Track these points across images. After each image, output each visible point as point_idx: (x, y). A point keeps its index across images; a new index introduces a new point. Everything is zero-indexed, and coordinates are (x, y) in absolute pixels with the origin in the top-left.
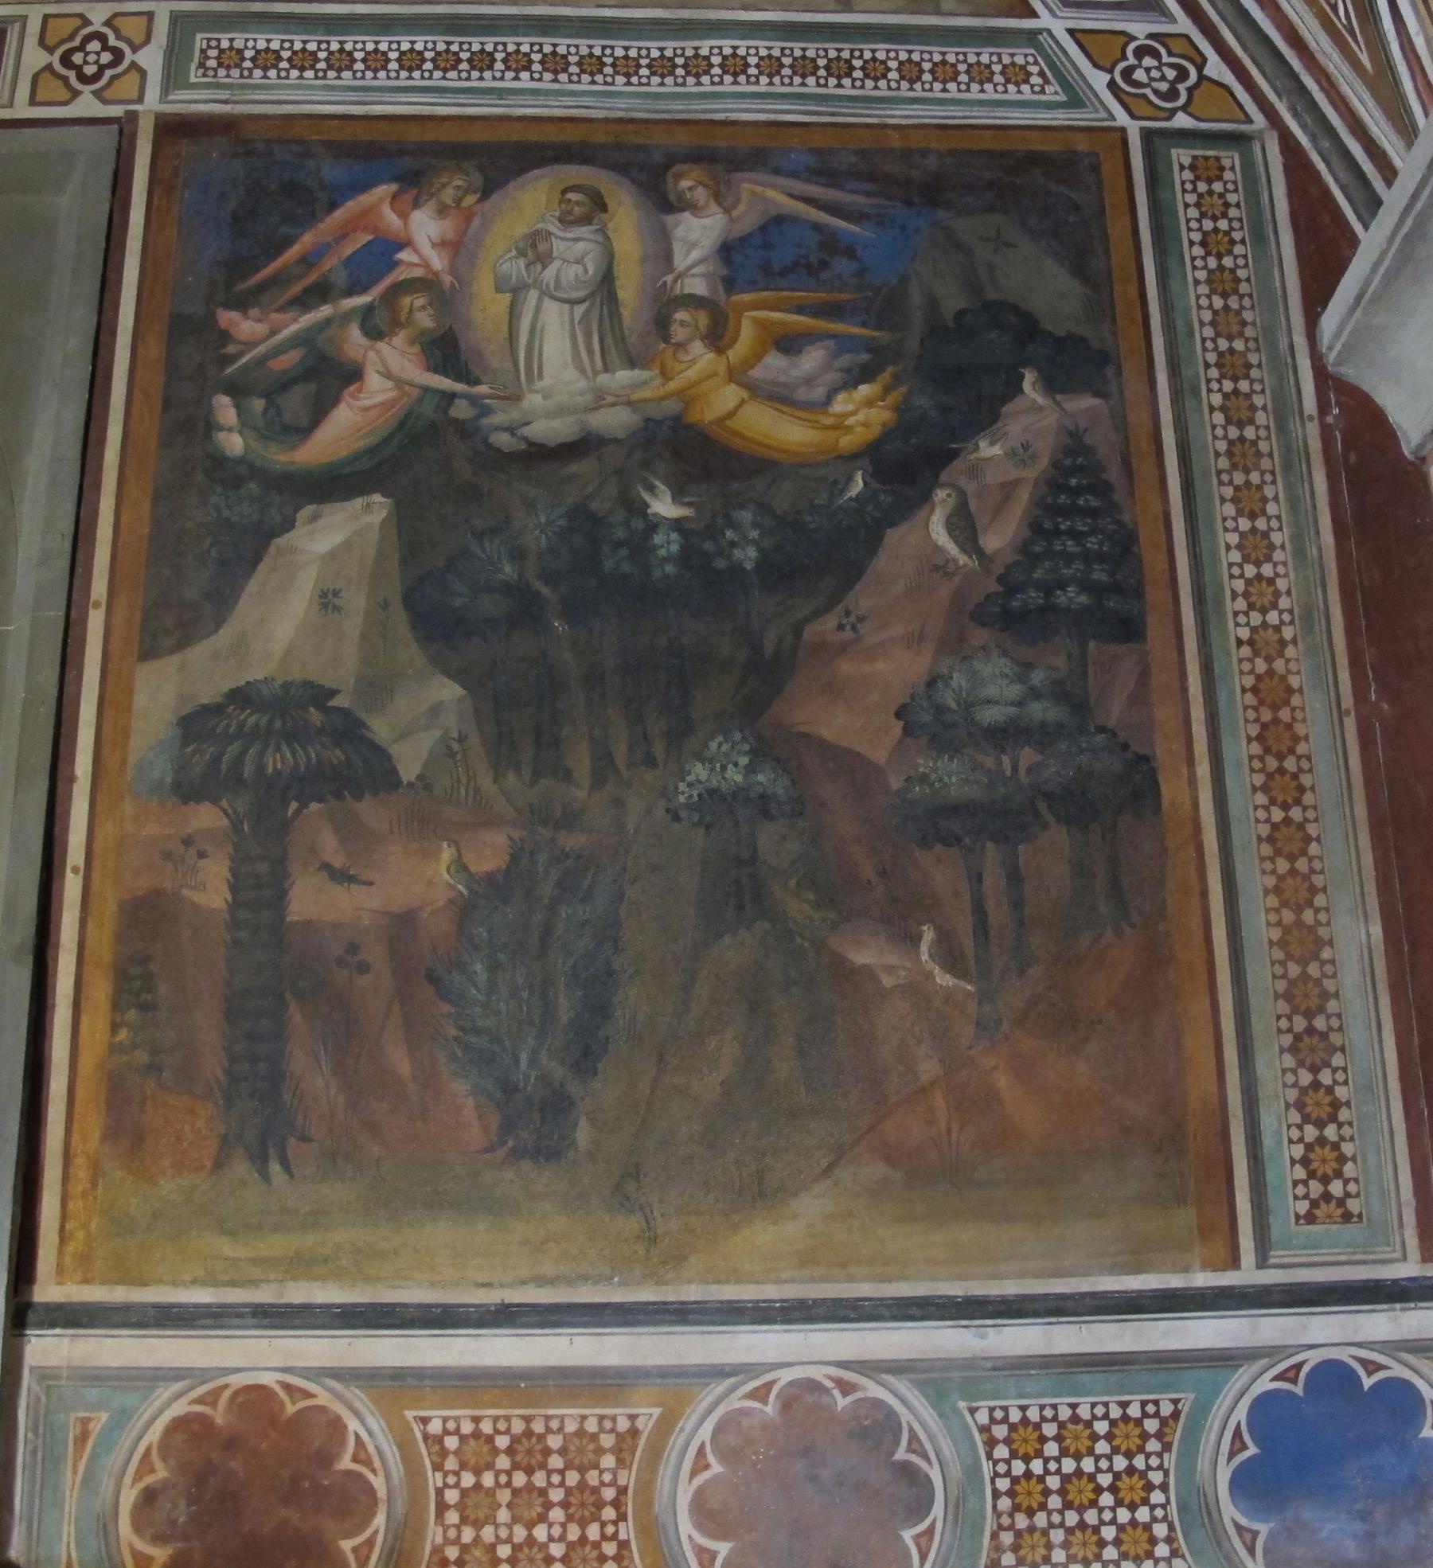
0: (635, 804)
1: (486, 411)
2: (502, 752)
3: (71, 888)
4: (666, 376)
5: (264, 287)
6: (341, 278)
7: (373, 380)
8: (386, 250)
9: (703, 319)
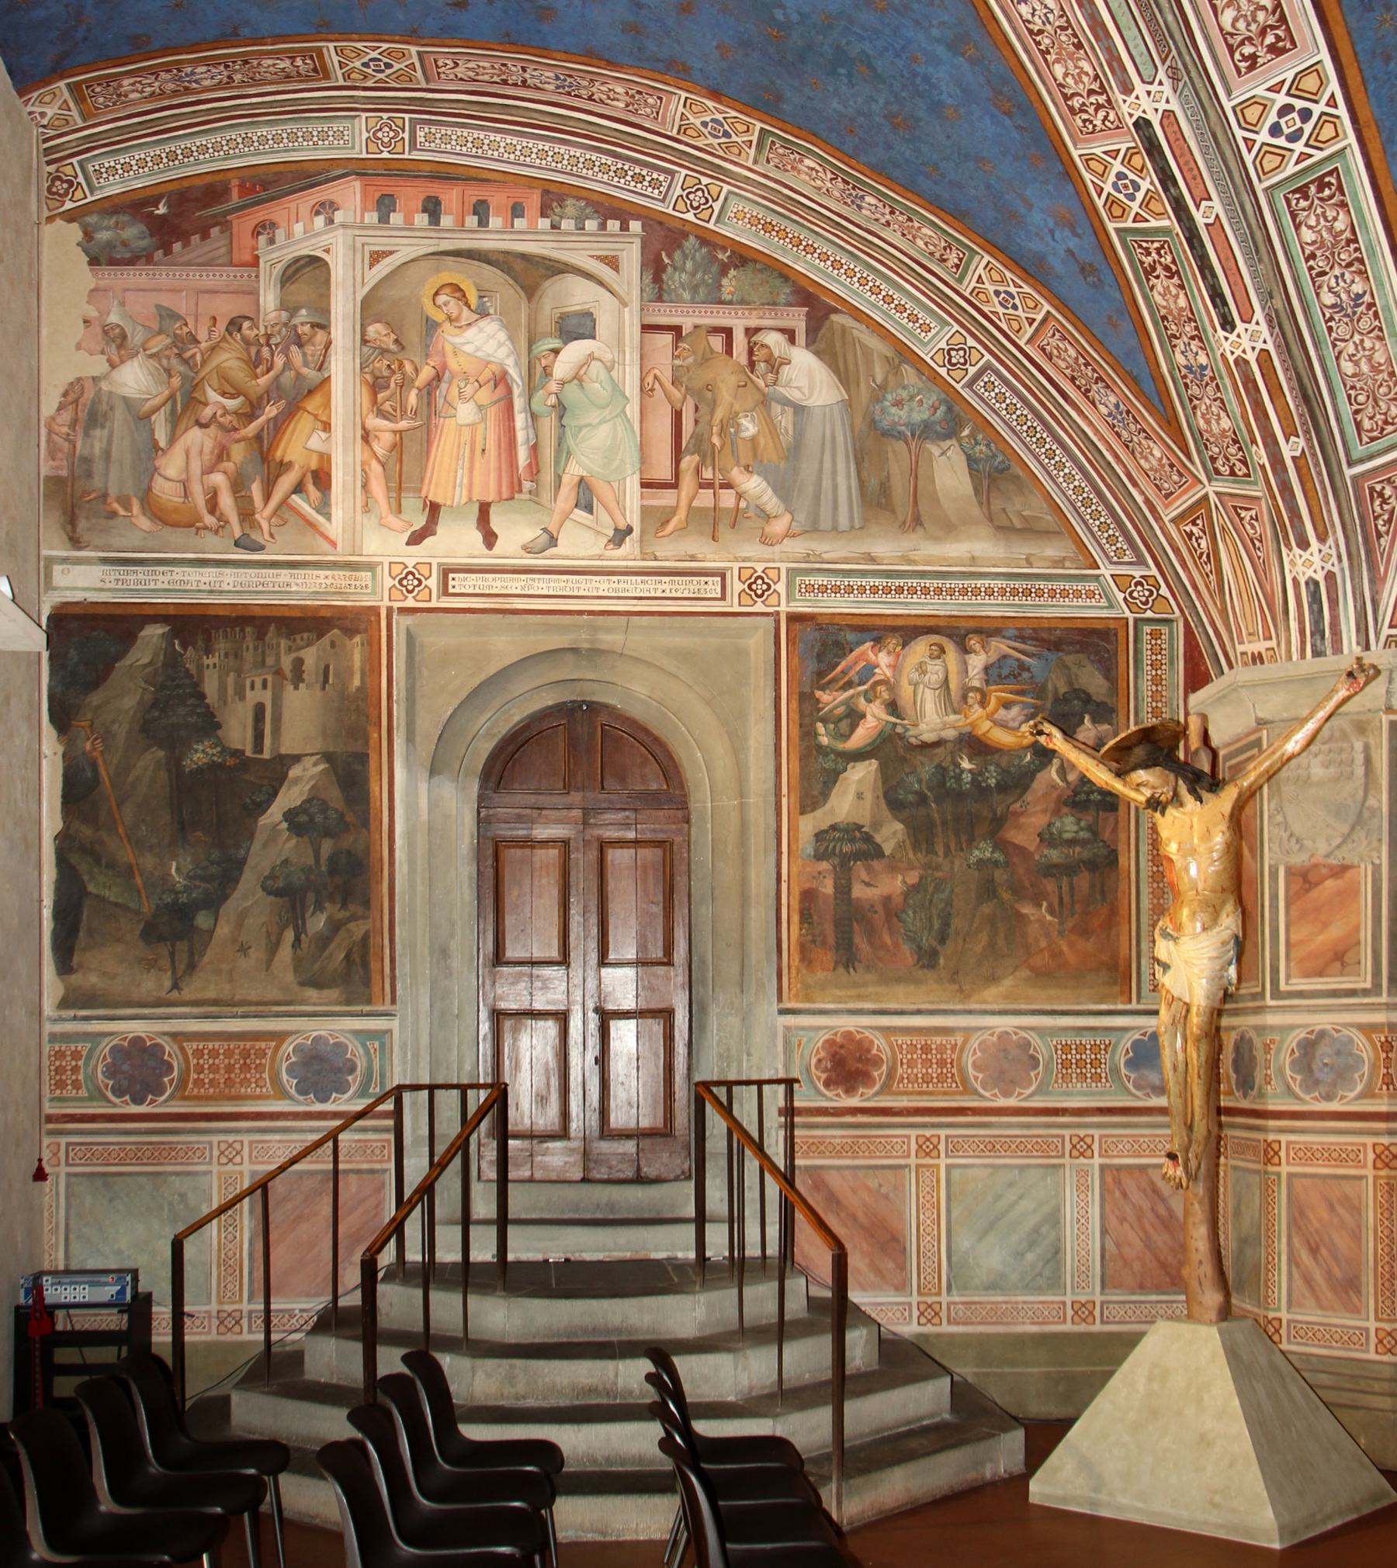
0: (957, 863)
1: (907, 730)
2: (916, 846)
3: (784, 886)
4: (966, 717)
5: (829, 682)
6: (856, 679)
7: (869, 717)
8: (871, 668)
9: (979, 697)
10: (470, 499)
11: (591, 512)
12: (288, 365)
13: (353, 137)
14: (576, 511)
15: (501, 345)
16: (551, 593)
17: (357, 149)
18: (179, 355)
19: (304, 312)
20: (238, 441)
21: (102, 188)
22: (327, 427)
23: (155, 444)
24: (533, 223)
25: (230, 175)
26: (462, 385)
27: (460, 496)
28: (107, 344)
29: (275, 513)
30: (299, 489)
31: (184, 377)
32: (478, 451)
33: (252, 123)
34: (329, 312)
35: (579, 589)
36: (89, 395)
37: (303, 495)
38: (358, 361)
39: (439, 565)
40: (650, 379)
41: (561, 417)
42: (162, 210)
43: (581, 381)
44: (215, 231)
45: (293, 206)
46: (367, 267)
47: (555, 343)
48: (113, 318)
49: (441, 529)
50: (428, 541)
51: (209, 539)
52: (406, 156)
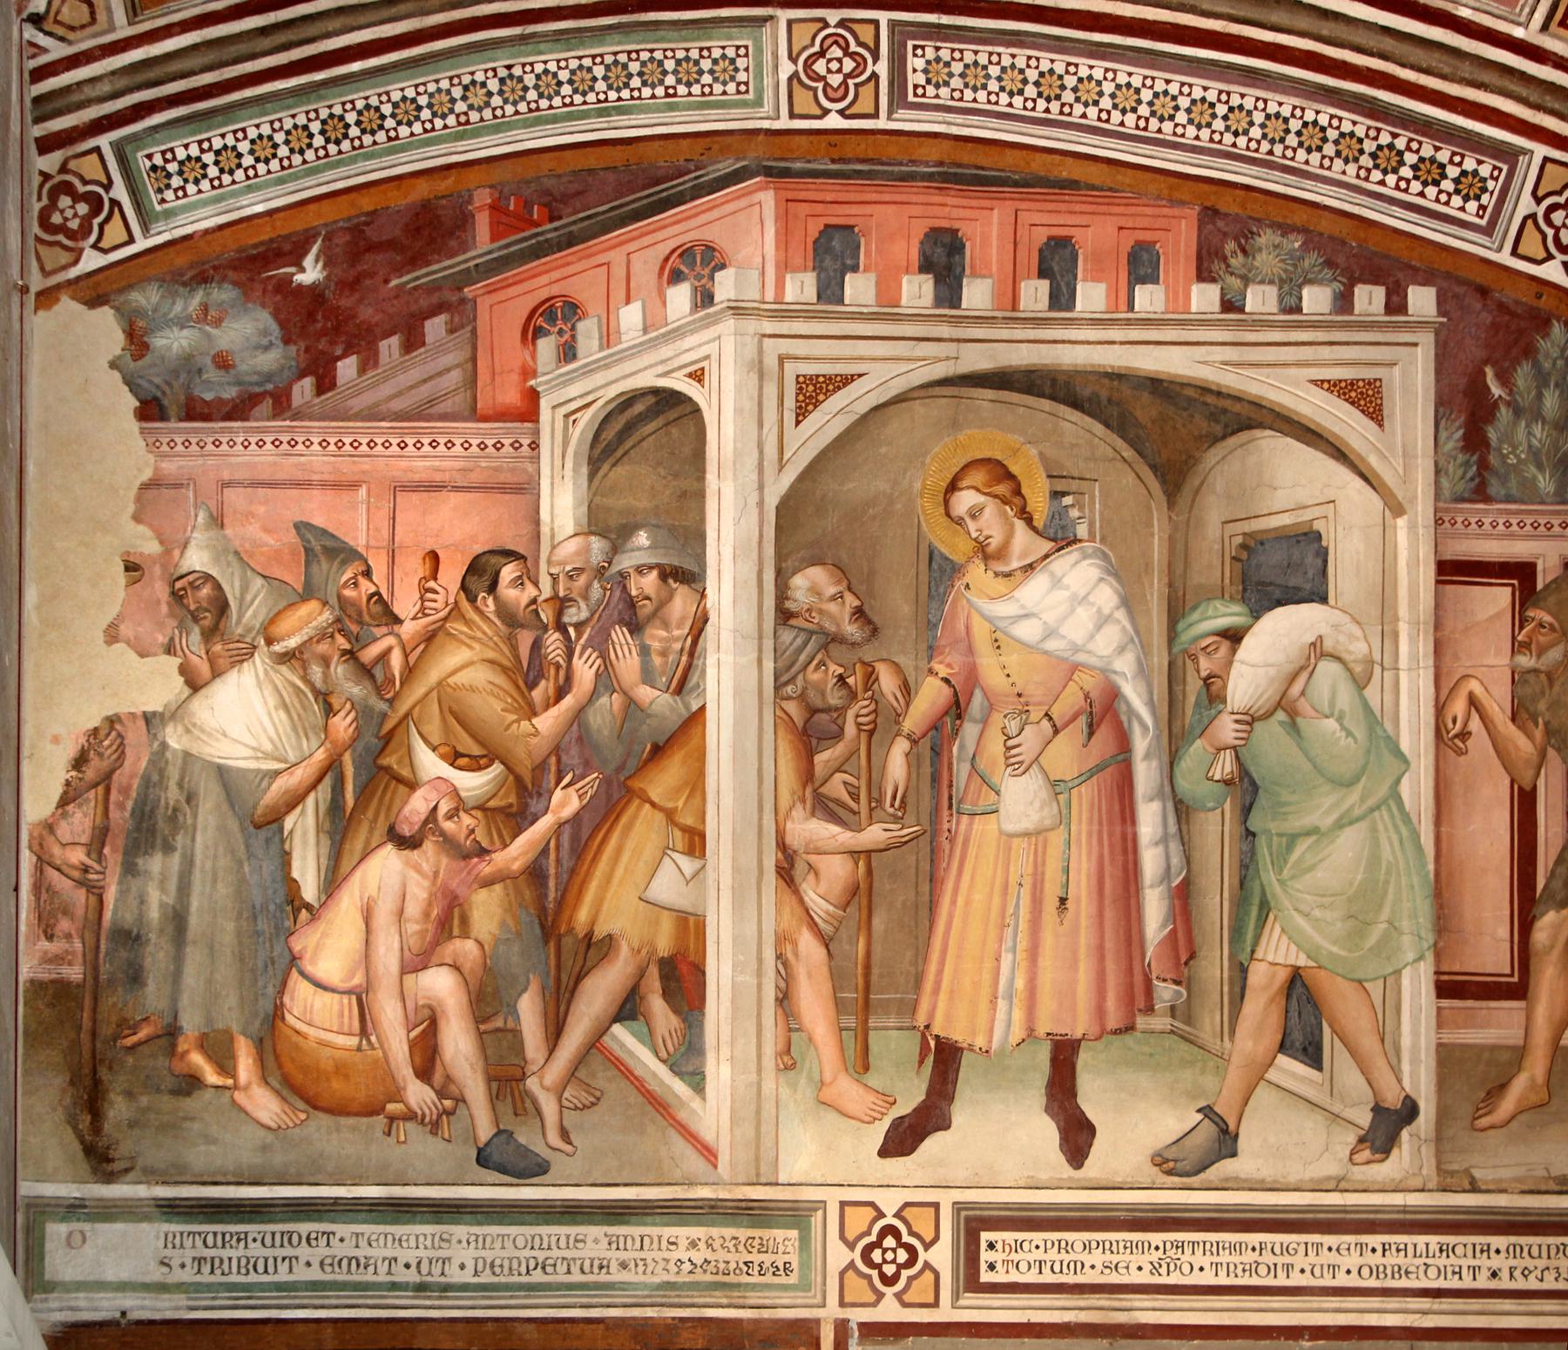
10: (1031, 1031)
11: (1317, 1063)
12: (606, 679)
13: (759, 76)
14: (1282, 1060)
15: (1103, 621)
16: (1223, 1280)
17: (768, 108)
18: (350, 655)
19: (642, 538)
20: (488, 883)
21: (169, 214)
22: (696, 843)
23: (292, 887)
24: (1178, 298)
25: (473, 176)
26: (1013, 727)
27: (1007, 1024)
28: (181, 626)
29: (572, 1075)
30: (628, 1008)
31: (364, 714)
32: (1051, 904)
33: (523, 39)
34: (701, 537)
35: (1288, 1268)
36: (137, 762)
37: (639, 1025)
38: (769, 666)
39: (958, 1207)
40: (1459, 707)
41: (1246, 811)
42: (311, 273)
43: (1293, 714)
44: (435, 327)
45: (617, 257)
46: (790, 417)
47: (1227, 615)
48: (196, 559)
49: (960, 1113)
50: (933, 1144)
51: (418, 1146)
52: (882, 123)
